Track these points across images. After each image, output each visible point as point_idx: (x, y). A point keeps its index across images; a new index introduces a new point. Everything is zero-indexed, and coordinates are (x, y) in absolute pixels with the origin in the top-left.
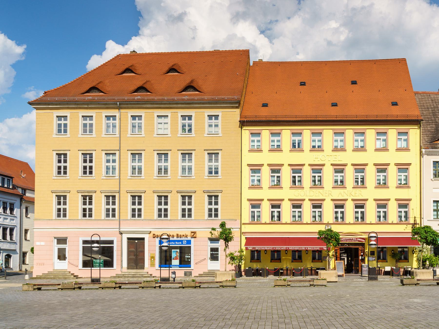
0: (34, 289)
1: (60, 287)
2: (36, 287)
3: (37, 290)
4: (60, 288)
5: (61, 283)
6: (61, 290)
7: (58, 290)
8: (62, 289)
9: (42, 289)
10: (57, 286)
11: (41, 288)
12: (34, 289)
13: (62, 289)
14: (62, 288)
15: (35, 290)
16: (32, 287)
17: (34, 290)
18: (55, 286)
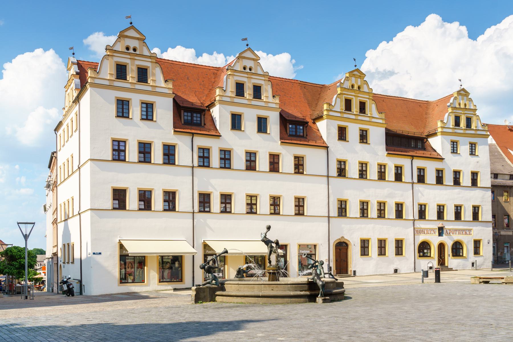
0: (480, 282)
1: (503, 281)
2: (481, 280)
3: (483, 283)
4: (504, 282)
5: (505, 277)
6: (505, 284)
7: (502, 284)
8: (506, 283)
9: (490, 282)
10: (500, 280)
11: (490, 281)
12: (480, 282)
13: (506, 283)
14: (506, 282)
15: (481, 283)
16: (478, 280)
17: (480, 283)
18: (499, 280)
